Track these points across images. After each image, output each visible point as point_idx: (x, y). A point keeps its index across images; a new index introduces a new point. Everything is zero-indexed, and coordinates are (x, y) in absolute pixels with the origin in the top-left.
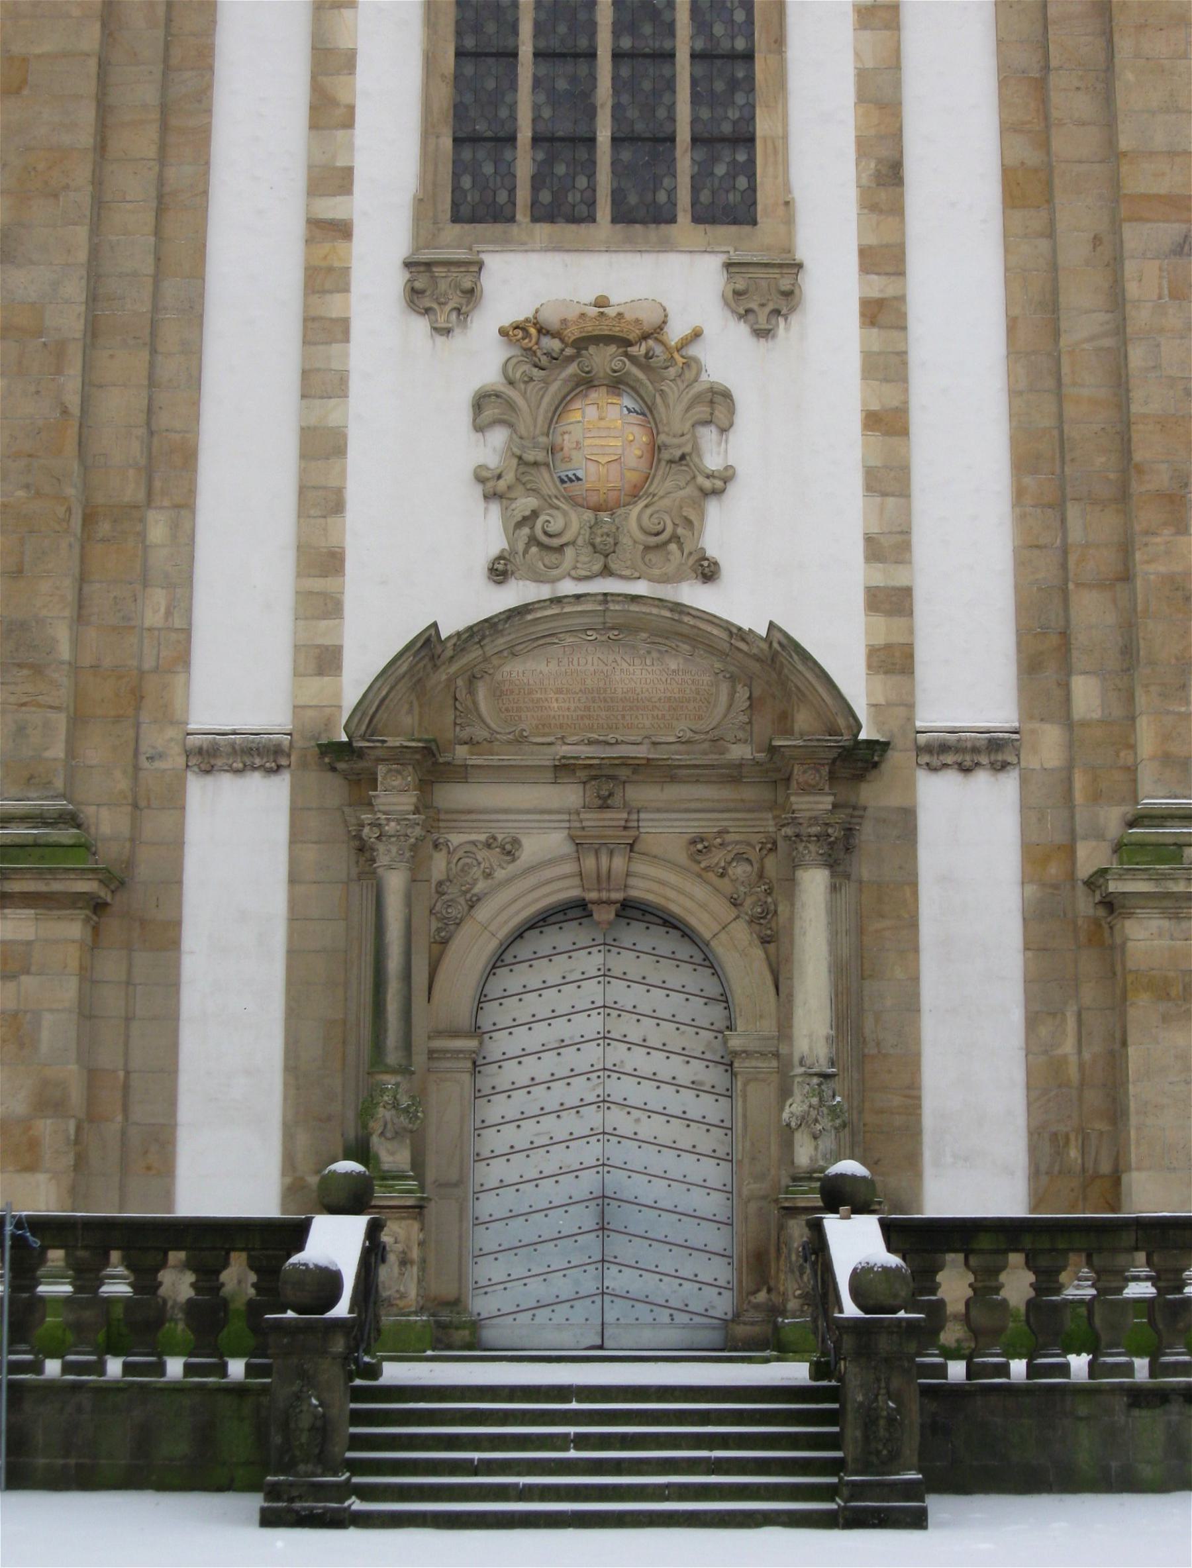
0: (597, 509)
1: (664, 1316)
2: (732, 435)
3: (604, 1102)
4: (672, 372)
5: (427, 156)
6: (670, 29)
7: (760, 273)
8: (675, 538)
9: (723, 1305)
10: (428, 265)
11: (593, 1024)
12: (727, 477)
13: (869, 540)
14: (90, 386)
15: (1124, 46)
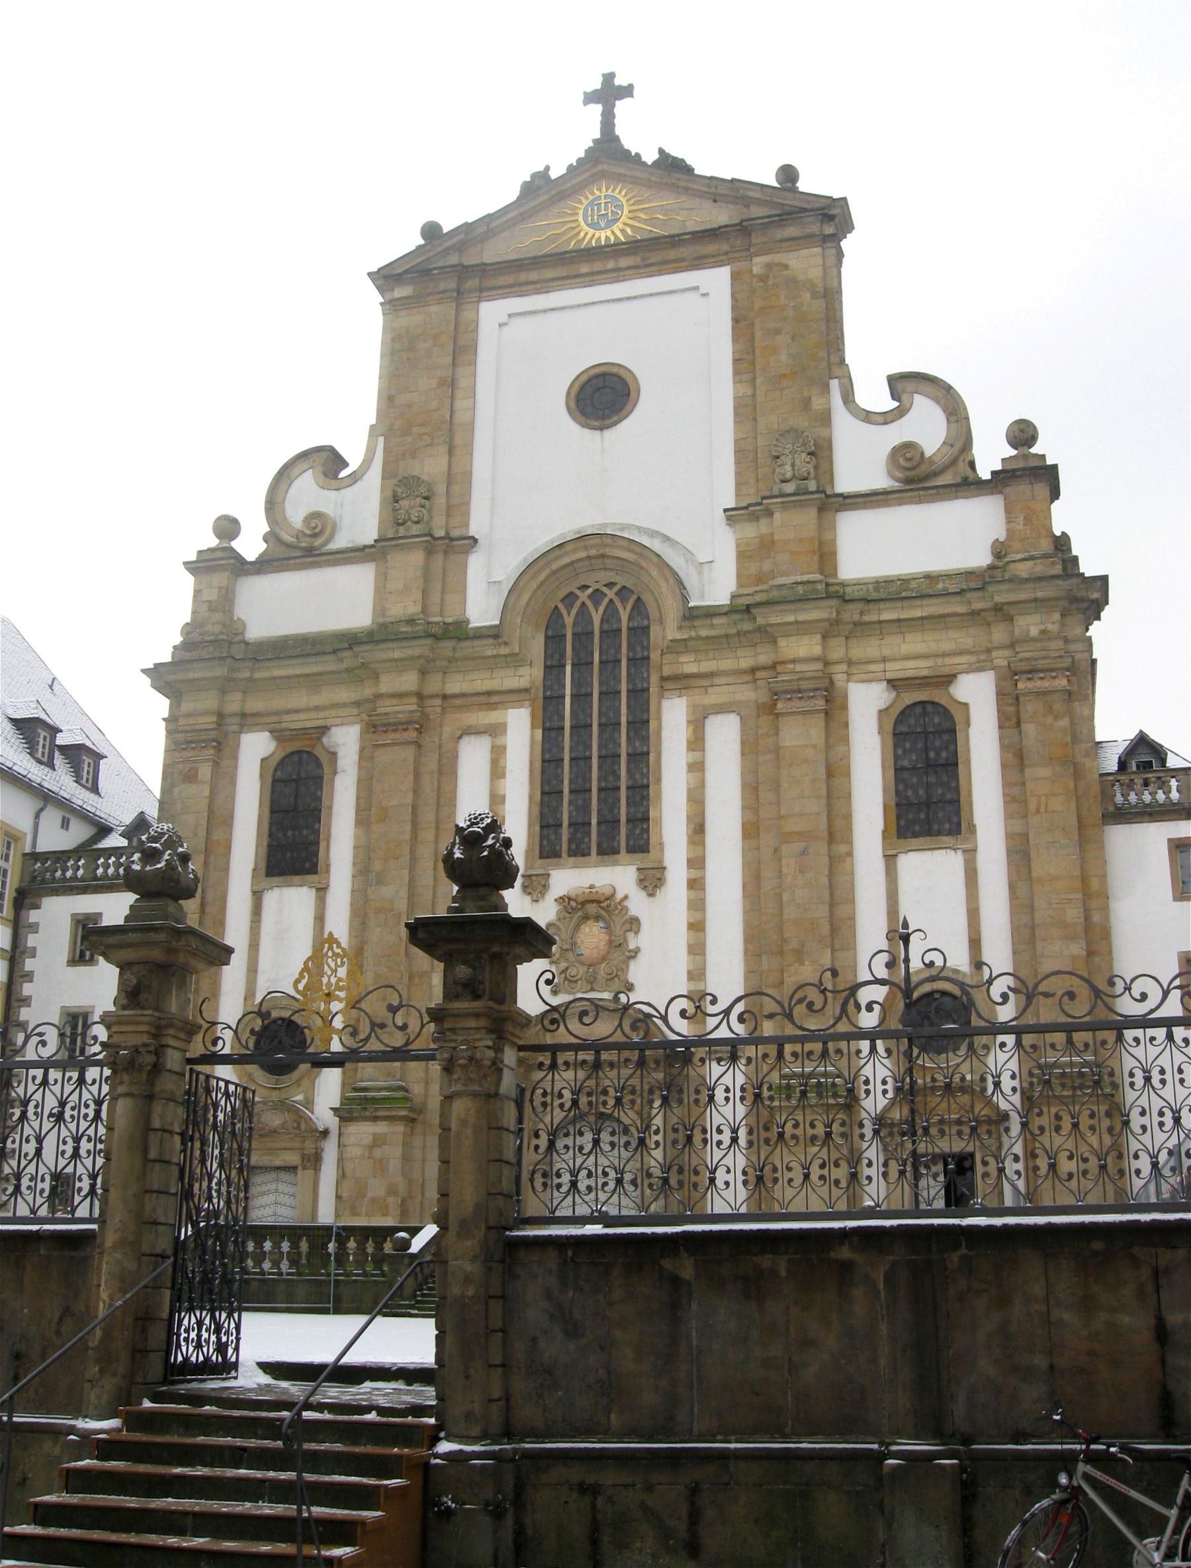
0: (590, 966)
2: (641, 935)
4: (617, 912)
6: (619, 778)
7: (650, 872)
8: (617, 975)
10: (530, 876)
12: (637, 951)
13: (689, 972)
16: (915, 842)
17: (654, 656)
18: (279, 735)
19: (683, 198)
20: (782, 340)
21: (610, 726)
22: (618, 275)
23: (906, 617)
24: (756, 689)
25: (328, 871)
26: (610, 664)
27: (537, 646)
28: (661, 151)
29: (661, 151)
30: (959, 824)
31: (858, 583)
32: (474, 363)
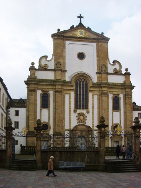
17: (88, 88)
18: (42, 91)
21: (83, 95)
22: (83, 41)
26: (83, 88)
27: (74, 85)
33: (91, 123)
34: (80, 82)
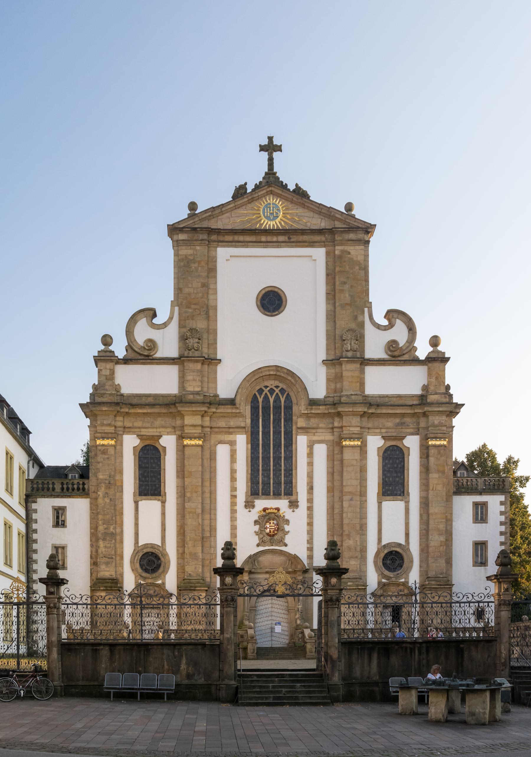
1: (279, 643)
3: (272, 616)
5: (247, 486)
6: (281, 466)
8: (281, 541)
9: (287, 642)
11: (270, 606)
12: (289, 532)
13: (308, 541)
14: (203, 520)
15: (345, 469)
16: (388, 498)
17: (294, 418)
18: (141, 437)
19: (306, 211)
20: (347, 287)
22: (278, 244)
23: (391, 412)
24: (333, 435)
25: (165, 495)
26: (277, 421)
27: (247, 410)
28: (297, 185)
29: (297, 185)
30: (403, 492)
31: (373, 397)
32: (215, 277)
33: (305, 546)
34: (266, 398)
